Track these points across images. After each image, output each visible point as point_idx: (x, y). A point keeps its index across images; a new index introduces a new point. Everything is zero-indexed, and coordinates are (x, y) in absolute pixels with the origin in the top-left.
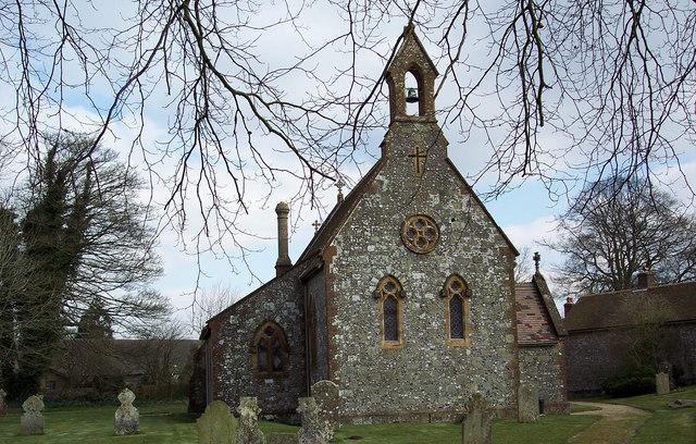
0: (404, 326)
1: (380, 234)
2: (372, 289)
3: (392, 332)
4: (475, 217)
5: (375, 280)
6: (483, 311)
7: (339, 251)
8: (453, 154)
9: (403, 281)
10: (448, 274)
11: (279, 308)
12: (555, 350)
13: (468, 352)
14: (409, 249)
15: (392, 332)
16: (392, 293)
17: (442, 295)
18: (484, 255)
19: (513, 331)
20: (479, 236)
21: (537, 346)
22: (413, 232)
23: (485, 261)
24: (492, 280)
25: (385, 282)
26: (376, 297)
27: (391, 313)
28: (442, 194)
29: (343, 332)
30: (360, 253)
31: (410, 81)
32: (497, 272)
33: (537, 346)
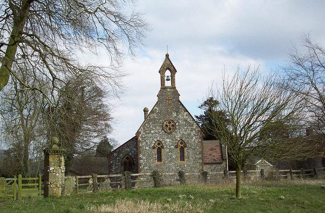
0: (163, 157)
1: (156, 127)
2: (153, 145)
3: (160, 159)
4: (189, 120)
5: (154, 142)
6: (191, 151)
7: (142, 133)
8: (181, 99)
9: (163, 142)
10: (179, 139)
11: (131, 150)
12: (223, 165)
13: (186, 166)
14: (165, 132)
15: (160, 159)
16: (160, 146)
17: (176, 147)
18: (191, 132)
19: (202, 158)
20: (190, 126)
21: (216, 163)
22: (167, 126)
23: (192, 135)
24: (194, 141)
25: (157, 143)
26: (154, 148)
27: (182, 150)
28: (177, 112)
29: (143, 160)
30: (149, 133)
31: (168, 73)
32: (196, 138)
33: (216, 163)
